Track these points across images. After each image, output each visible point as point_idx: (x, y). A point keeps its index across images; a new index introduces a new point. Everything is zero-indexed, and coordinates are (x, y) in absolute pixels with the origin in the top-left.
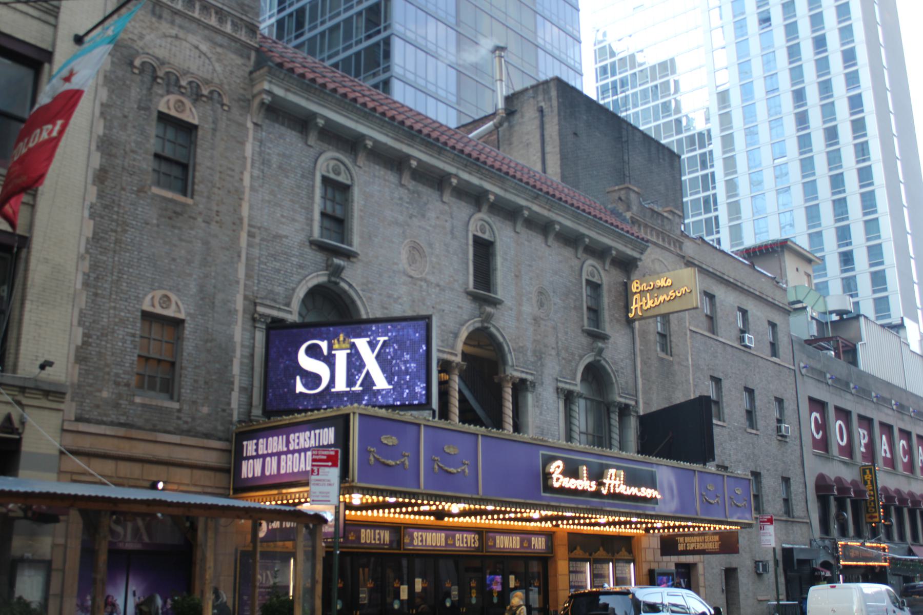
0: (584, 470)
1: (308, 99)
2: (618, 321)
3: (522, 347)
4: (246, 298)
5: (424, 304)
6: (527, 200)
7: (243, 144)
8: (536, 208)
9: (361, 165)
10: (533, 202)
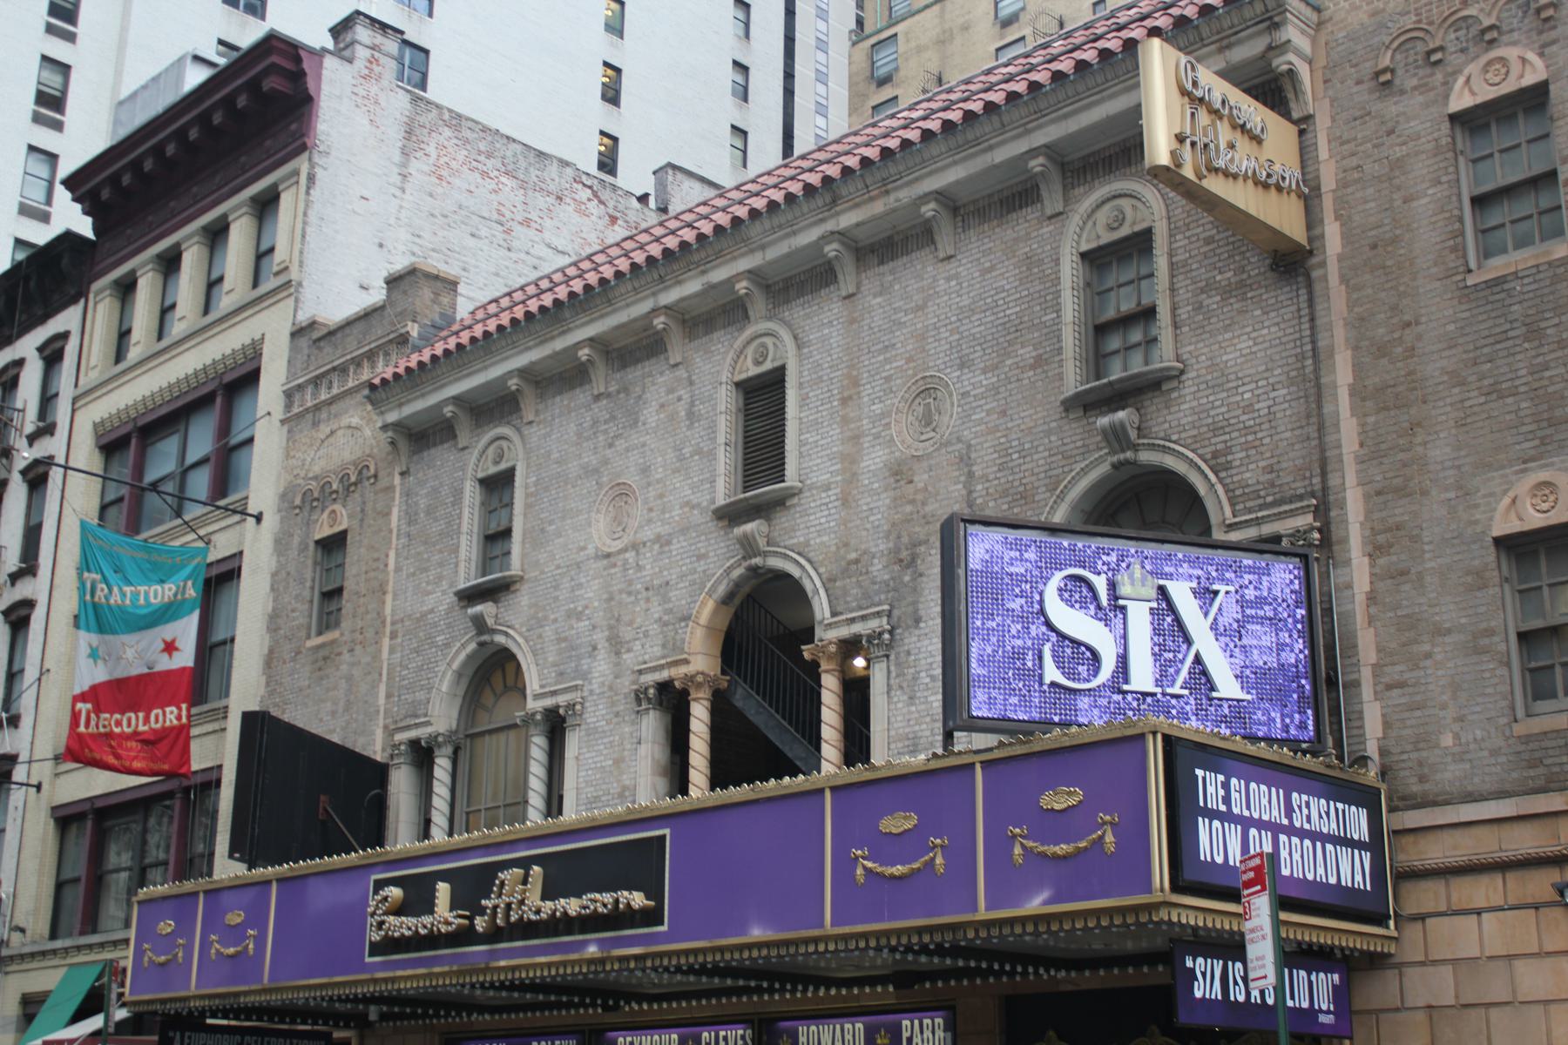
0: (443, 890)
1: (423, 395)
2: (1227, 292)
3: (857, 561)
4: (386, 727)
5: (629, 594)
6: (822, 220)
7: (388, 514)
8: (847, 220)
9: (531, 418)
10: (838, 214)
